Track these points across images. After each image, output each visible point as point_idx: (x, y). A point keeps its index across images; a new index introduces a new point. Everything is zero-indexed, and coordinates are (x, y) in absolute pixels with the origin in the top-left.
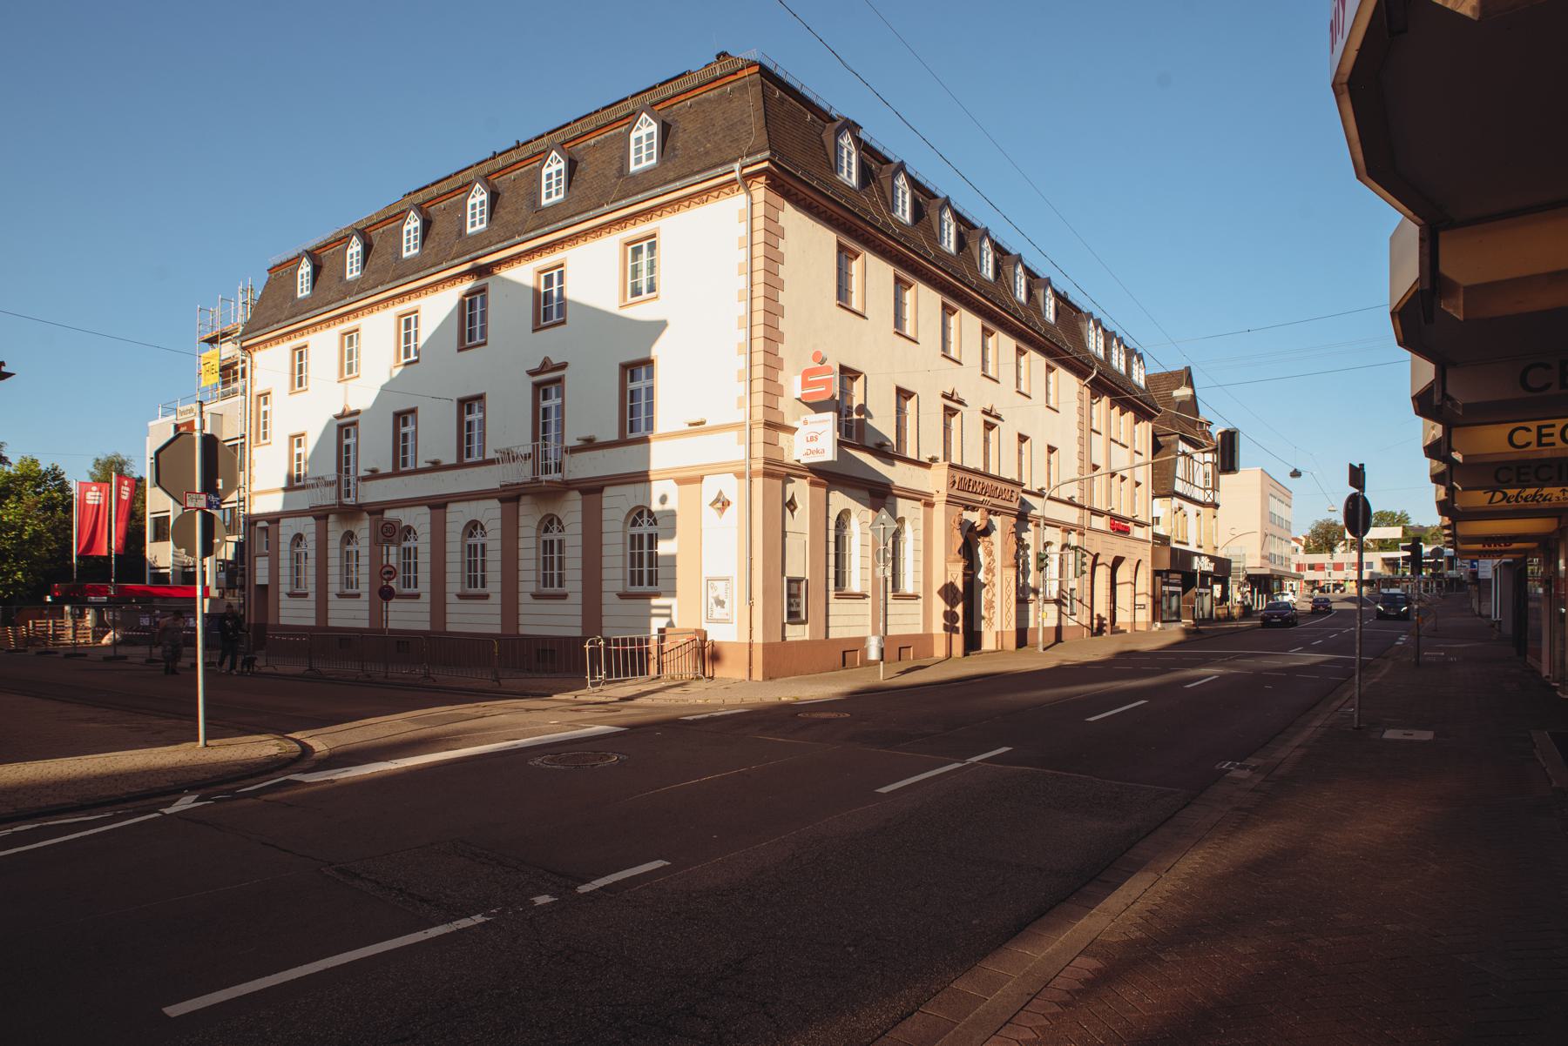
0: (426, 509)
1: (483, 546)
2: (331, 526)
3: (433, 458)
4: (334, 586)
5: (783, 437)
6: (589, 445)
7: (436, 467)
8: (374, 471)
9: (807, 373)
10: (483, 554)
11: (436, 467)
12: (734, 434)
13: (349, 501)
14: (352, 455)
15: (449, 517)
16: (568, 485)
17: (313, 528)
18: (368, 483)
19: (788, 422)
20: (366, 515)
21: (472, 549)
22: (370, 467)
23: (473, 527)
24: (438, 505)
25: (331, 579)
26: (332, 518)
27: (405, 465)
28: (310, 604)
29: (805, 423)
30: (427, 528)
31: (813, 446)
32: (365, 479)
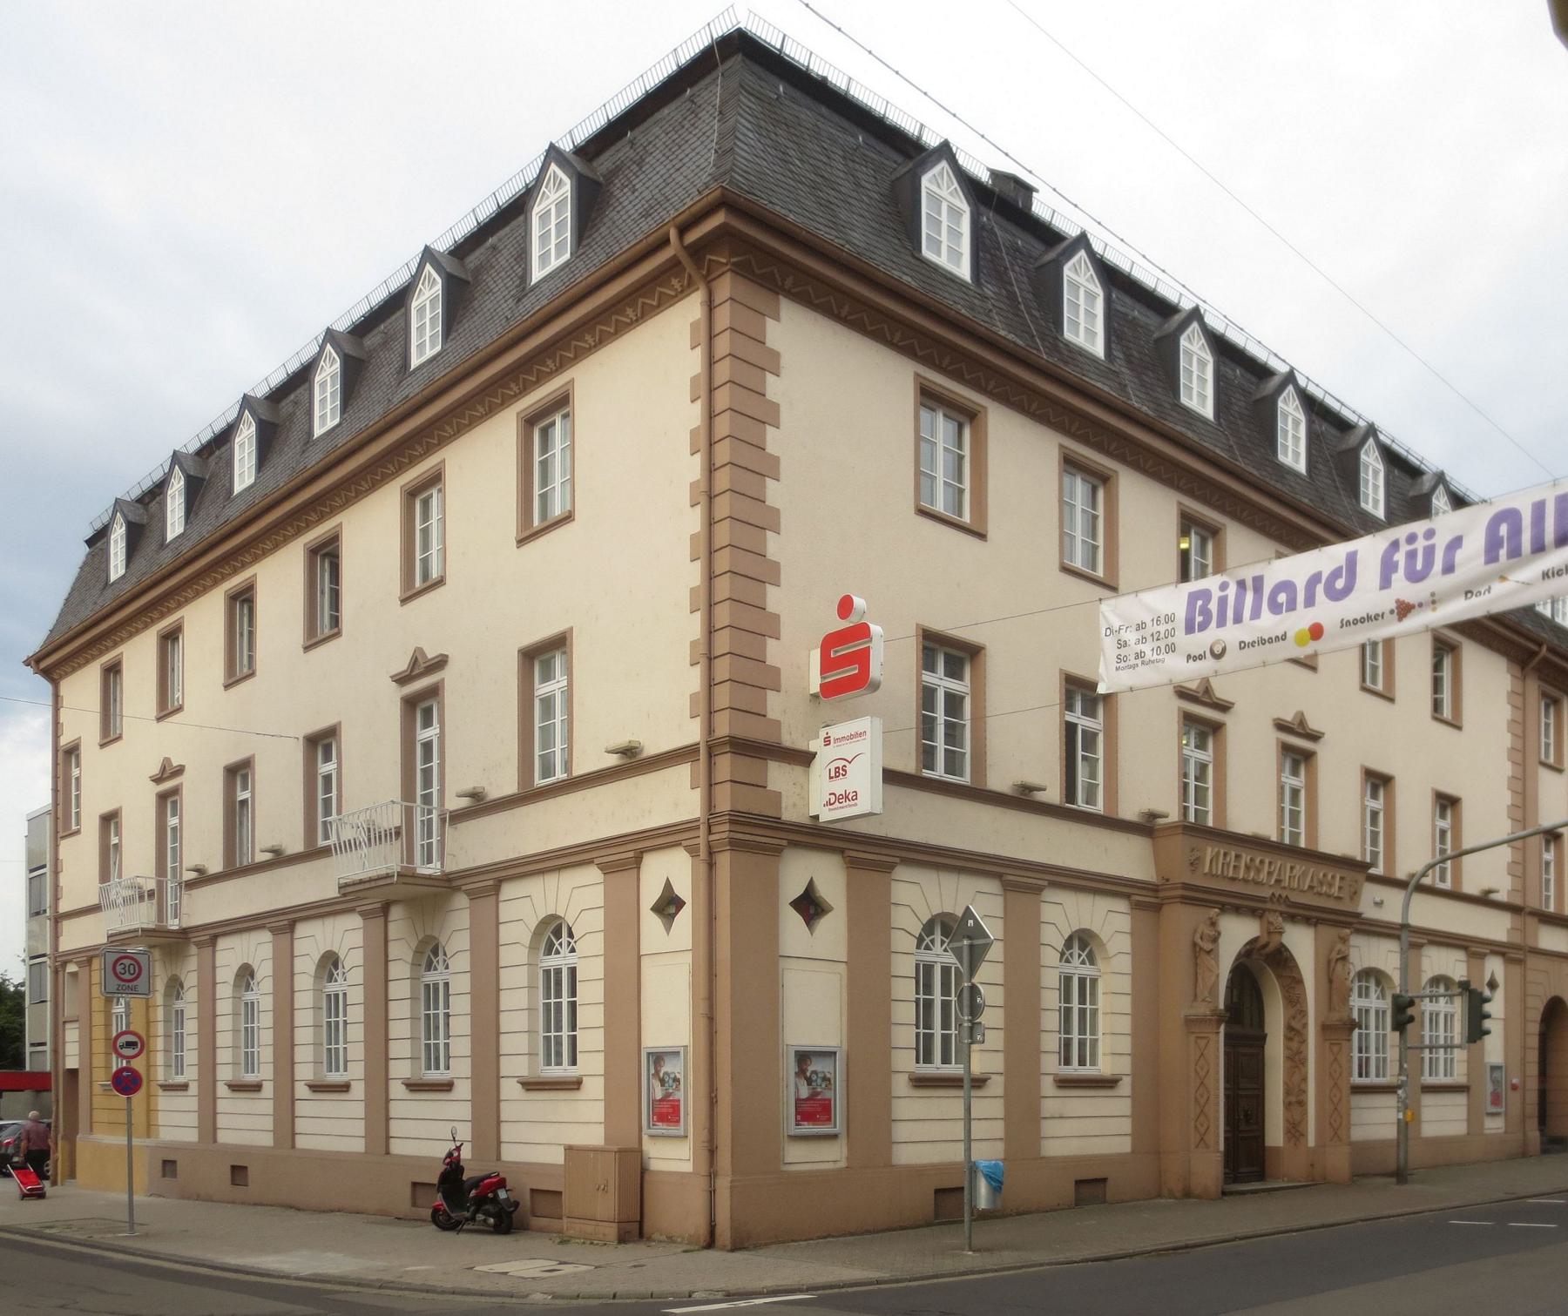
0: (592, 874)
1: (573, 971)
2: (395, 929)
3: (622, 740)
4: (517, 1060)
5: (779, 776)
6: (480, 806)
7: (280, 859)
8: (629, 752)
9: (830, 642)
10: (573, 993)
11: (280, 859)
12: (683, 772)
13: (173, 924)
14: (559, 718)
15: (506, 912)
16: (449, 883)
17: (357, 938)
18: (195, 892)
19: (789, 739)
20: (193, 950)
21: (552, 980)
22: (468, 786)
23: (553, 931)
24: (284, 923)
25: (508, 1044)
26: (396, 913)
27: (547, 770)
28: (264, 1104)
29: (827, 741)
30: (597, 920)
31: (839, 786)
32: (458, 817)
